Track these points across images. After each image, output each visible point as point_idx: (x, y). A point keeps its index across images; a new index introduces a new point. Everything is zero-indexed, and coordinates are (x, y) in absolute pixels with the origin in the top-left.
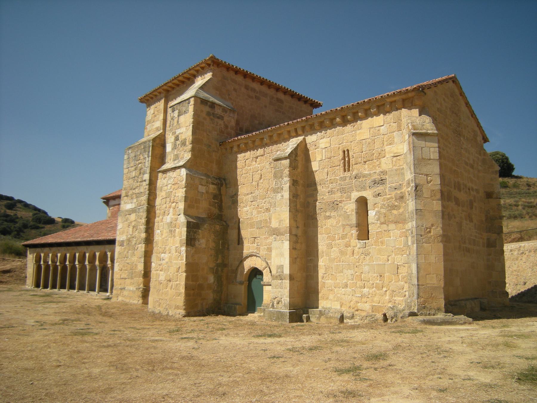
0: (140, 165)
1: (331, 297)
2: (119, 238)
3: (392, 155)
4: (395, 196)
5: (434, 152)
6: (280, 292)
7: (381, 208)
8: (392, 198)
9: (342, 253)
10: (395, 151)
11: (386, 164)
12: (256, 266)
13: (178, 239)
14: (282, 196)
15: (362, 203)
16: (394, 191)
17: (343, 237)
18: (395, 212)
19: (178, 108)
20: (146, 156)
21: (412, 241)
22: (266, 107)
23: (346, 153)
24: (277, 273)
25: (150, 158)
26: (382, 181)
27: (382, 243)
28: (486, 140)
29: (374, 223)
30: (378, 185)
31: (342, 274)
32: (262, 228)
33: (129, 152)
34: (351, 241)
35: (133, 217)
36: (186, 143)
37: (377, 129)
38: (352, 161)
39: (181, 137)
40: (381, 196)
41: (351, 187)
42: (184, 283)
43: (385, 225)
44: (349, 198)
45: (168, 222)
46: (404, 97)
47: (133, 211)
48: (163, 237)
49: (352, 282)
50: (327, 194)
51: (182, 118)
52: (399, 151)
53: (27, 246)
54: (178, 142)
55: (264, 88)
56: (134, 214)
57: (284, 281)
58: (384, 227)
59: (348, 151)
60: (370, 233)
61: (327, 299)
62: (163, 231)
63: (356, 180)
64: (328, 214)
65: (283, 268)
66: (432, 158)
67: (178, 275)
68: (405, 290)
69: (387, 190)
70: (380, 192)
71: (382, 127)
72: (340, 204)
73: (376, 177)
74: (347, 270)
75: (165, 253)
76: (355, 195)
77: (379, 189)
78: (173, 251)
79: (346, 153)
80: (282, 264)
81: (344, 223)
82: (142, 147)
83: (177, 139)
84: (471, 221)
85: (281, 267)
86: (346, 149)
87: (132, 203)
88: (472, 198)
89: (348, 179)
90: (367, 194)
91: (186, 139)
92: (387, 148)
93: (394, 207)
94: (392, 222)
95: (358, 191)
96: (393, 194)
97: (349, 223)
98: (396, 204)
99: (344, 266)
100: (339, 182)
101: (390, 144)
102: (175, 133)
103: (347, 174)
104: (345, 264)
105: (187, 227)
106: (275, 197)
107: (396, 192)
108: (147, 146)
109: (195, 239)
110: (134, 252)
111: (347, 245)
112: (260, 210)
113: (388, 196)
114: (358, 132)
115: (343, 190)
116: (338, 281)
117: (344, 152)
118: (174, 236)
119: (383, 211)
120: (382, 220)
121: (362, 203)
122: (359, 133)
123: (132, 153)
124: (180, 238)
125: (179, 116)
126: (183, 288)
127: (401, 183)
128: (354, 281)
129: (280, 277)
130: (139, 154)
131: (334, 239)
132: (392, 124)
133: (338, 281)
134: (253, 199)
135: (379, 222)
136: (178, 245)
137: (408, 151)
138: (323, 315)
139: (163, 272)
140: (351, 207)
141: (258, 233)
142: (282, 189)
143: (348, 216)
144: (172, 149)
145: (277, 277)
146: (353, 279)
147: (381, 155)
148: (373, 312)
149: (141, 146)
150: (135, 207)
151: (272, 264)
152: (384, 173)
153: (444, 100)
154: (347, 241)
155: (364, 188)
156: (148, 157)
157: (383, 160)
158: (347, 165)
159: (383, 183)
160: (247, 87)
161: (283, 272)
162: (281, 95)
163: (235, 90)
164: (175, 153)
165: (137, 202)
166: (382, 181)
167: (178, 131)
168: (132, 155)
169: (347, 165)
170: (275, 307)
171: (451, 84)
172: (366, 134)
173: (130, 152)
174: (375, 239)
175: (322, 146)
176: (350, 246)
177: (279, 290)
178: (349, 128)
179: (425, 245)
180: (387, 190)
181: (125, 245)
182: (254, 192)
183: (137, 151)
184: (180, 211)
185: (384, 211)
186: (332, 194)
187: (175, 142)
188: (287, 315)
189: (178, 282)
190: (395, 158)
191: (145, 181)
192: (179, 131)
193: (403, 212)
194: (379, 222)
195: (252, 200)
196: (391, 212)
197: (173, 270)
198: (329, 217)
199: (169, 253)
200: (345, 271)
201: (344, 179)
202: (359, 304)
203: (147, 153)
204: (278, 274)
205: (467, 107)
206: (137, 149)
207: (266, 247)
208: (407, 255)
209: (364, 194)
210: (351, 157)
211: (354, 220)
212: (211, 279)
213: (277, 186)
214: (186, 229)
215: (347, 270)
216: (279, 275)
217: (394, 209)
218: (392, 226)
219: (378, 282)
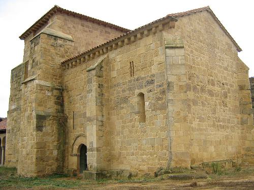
1: (125, 162)
3: (158, 63)
5: (181, 59)
9: (131, 132)
10: (160, 60)
11: (154, 70)
15: (142, 95)
17: (131, 121)
18: (160, 102)
26: (152, 82)
27: (153, 124)
28: (239, 50)
38: (135, 70)
39: (36, 61)
41: (135, 87)
44: (134, 94)
46: (163, 22)
52: (162, 60)
61: (123, 163)
66: (180, 63)
71: (152, 45)
76: (137, 92)
77: (150, 87)
78: (30, 135)
83: (33, 61)
84: (226, 105)
88: (227, 91)
90: (144, 91)
92: (155, 59)
93: (159, 99)
95: (138, 89)
101: (157, 56)
103: (132, 78)
114: (138, 49)
115: (130, 89)
116: (128, 151)
119: (153, 102)
140: (135, 100)
142: (92, 91)
147: (151, 64)
148: (149, 171)
152: (153, 76)
153: (198, 23)
155: (142, 87)
157: (153, 67)
158: (132, 73)
163: (73, 27)
166: (152, 82)
169: (132, 73)
171: (205, 14)
175: (118, 60)
178: (132, 47)
179: (176, 124)
190: (159, 66)
193: (164, 102)
197: (29, 147)
198: (123, 108)
200: (132, 144)
201: (130, 81)
209: (142, 91)
212: (55, 153)
218: (159, 112)
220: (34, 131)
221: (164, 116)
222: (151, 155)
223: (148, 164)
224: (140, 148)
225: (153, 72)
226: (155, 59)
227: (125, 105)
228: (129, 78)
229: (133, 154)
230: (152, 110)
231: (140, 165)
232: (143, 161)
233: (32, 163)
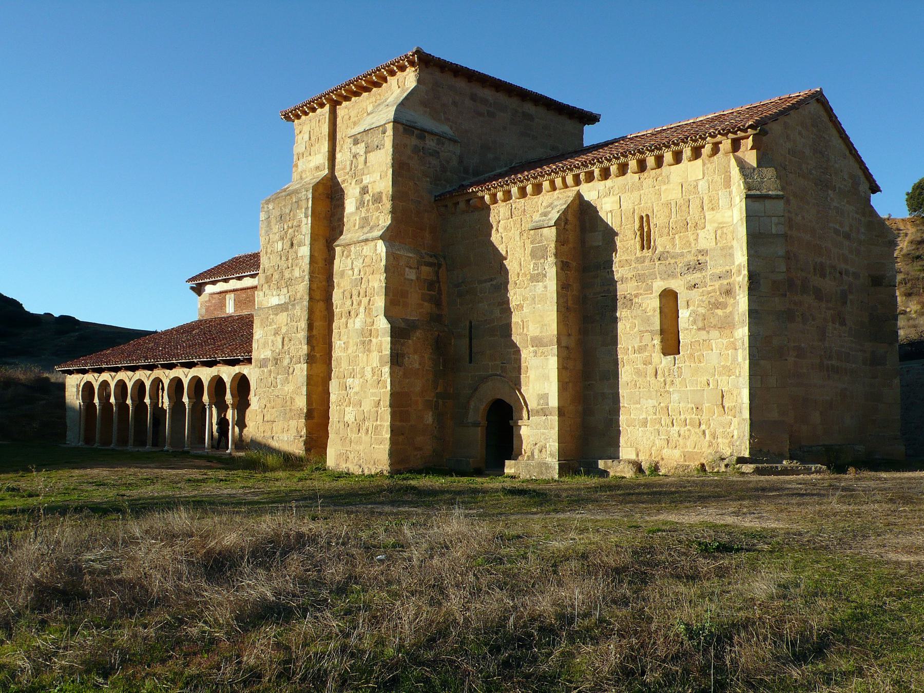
6: (543, 434)
7: (699, 306)
8: (714, 291)
10: (720, 220)
11: (705, 240)
12: (499, 397)
14: (545, 287)
15: (669, 298)
16: (718, 281)
18: (720, 312)
19: (365, 139)
20: (302, 215)
21: (743, 356)
22: (505, 128)
24: (538, 405)
25: (310, 218)
26: (699, 266)
28: (875, 189)
30: (694, 272)
31: (638, 406)
33: (268, 208)
34: (653, 355)
35: (283, 318)
36: (381, 198)
40: (698, 288)
42: (389, 423)
43: (704, 332)
44: (650, 289)
45: (356, 327)
47: (282, 308)
48: (350, 351)
49: (654, 417)
51: (372, 156)
53: (64, 372)
54: (367, 197)
55: (502, 98)
56: (285, 314)
60: (681, 345)
62: (348, 342)
63: (659, 262)
65: (548, 398)
66: (774, 231)
69: (708, 280)
70: (697, 281)
73: (691, 258)
74: (647, 400)
76: (659, 285)
77: (696, 277)
78: (368, 375)
81: (642, 329)
82: (294, 201)
83: (364, 191)
84: (843, 323)
85: (545, 397)
87: (278, 295)
88: (846, 287)
89: (647, 261)
91: (382, 193)
93: (717, 305)
94: (715, 327)
96: (717, 284)
97: (648, 328)
98: (721, 300)
99: (641, 394)
100: (634, 265)
104: (644, 391)
105: (392, 336)
106: (533, 288)
107: (720, 282)
108: (304, 198)
109: (403, 356)
110: (287, 378)
111: (647, 363)
113: (710, 289)
117: (642, 218)
118: (369, 351)
119: (702, 310)
120: (700, 325)
121: (669, 298)
122: (666, 189)
124: (380, 354)
125: (366, 153)
126: (386, 432)
127: (728, 268)
128: (658, 416)
129: (544, 412)
130: (288, 211)
137: (740, 222)
142: (545, 276)
143: (648, 319)
144: (357, 208)
145: (538, 412)
149: (291, 198)
151: (531, 391)
152: (701, 252)
153: (800, 133)
154: (647, 356)
155: (672, 275)
156: (306, 217)
157: (702, 234)
159: (700, 268)
160: (473, 98)
161: (548, 404)
162: (529, 108)
163: (455, 103)
164: (363, 215)
165: (289, 294)
166: (699, 266)
167: (366, 179)
168: (276, 213)
171: (814, 106)
172: (676, 191)
173: (271, 207)
176: (650, 363)
177: (542, 431)
182: (495, 278)
183: (284, 206)
184: (377, 310)
185: (703, 311)
187: (362, 197)
188: (554, 469)
189: (378, 423)
192: (368, 179)
193: (731, 313)
196: (713, 313)
200: (643, 401)
203: (303, 210)
204: (540, 407)
205: (841, 137)
206: (283, 203)
208: (736, 376)
210: (652, 225)
211: (656, 323)
212: (429, 418)
213: (536, 272)
214: (389, 338)
215: (647, 400)
217: (718, 308)
218: (714, 333)
219: (693, 416)
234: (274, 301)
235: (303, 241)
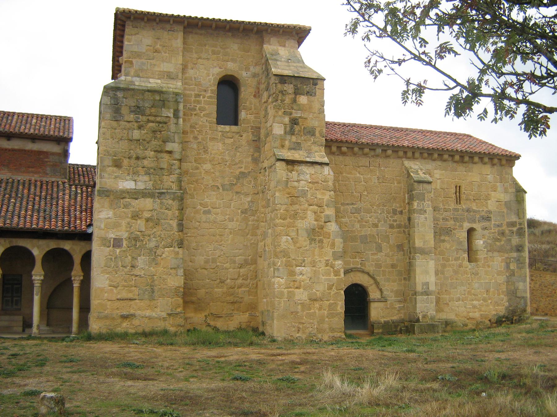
0: (151, 124)
2: (97, 231)
3: (496, 200)
4: (498, 231)
7: (488, 239)
8: (495, 232)
9: (456, 272)
11: (492, 205)
13: (330, 251)
17: (457, 259)
18: (498, 243)
20: (171, 115)
23: (458, 189)
24: (422, 289)
27: (489, 266)
29: (482, 250)
32: (368, 243)
37: (485, 176)
44: (461, 226)
49: (464, 296)
50: (441, 220)
54: (297, 128)
57: (429, 296)
58: (490, 254)
59: (460, 187)
64: (442, 238)
67: (330, 293)
68: (504, 301)
70: (487, 226)
72: (453, 231)
75: (304, 266)
76: (467, 225)
79: (458, 189)
80: (428, 281)
86: (458, 185)
94: (496, 251)
98: (499, 237)
102: (291, 114)
103: (458, 207)
111: (460, 266)
112: (364, 223)
113: (493, 231)
114: (470, 174)
115: (455, 220)
116: (452, 296)
117: (456, 187)
119: (489, 241)
123: (126, 98)
127: (502, 222)
131: (448, 260)
132: (496, 175)
133: (452, 296)
134: (355, 211)
135: (486, 250)
136: (329, 257)
138: (448, 325)
139: (302, 290)
141: (362, 248)
145: (422, 293)
146: (465, 295)
147: (488, 198)
148: (481, 319)
150: (146, 189)
152: (490, 212)
154: (460, 263)
155: (474, 221)
158: (458, 200)
161: (429, 289)
170: (421, 321)
174: (482, 262)
180: (492, 226)
181: (124, 245)
182: (355, 204)
183: (143, 100)
186: (446, 221)
189: (331, 302)
190: (497, 203)
191: (170, 152)
194: (486, 250)
195: (353, 211)
198: (444, 241)
199: (314, 267)
201: (456, 210)
202: (471, 314)
203: (172, 111)
207: (374, 263)
209: (474, 226)
216: (425, 291)
217: (497, 241)
218: (496, 254)
219: (485, 295)
220: (335, 259)
221: (503, 260)
222: (485, 300)
223: (481, 311)
224: (469, 293)
225: (490, 208)
226: (493, 194)
227: (447, 238)
228: (452, 205)
229: (458, 300)
230: (488, 251)
231: (469, 312)
232: (474, 307)
233: (331, 315)
234: (128, 185)
235: (172, 138)
